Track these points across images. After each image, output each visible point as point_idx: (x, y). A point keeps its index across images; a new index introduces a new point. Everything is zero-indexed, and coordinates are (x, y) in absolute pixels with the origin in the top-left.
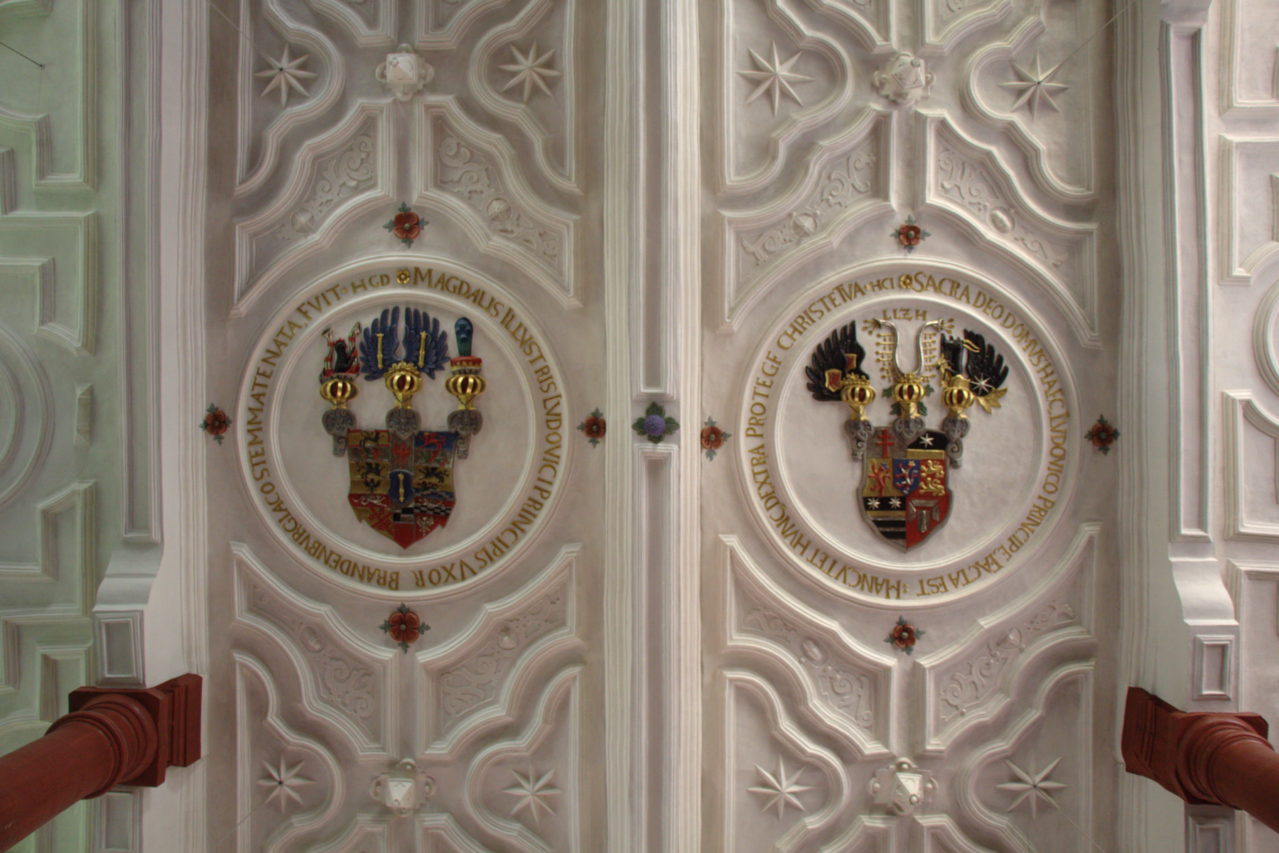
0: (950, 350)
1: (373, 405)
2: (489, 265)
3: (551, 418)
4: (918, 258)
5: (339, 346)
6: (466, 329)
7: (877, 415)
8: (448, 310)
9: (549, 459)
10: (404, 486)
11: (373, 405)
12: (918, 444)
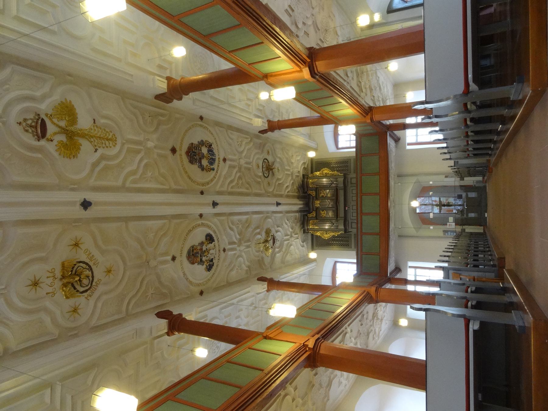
0: (212, 260)
1: (204, 150)
3: (203, 185)
4: (222, 252)
6: (213, 169)
7: (204, 248)
8: (215, 166)
9: (198, 184)
10: (193, 154)
11: (204, 150)
12: (201, 256)
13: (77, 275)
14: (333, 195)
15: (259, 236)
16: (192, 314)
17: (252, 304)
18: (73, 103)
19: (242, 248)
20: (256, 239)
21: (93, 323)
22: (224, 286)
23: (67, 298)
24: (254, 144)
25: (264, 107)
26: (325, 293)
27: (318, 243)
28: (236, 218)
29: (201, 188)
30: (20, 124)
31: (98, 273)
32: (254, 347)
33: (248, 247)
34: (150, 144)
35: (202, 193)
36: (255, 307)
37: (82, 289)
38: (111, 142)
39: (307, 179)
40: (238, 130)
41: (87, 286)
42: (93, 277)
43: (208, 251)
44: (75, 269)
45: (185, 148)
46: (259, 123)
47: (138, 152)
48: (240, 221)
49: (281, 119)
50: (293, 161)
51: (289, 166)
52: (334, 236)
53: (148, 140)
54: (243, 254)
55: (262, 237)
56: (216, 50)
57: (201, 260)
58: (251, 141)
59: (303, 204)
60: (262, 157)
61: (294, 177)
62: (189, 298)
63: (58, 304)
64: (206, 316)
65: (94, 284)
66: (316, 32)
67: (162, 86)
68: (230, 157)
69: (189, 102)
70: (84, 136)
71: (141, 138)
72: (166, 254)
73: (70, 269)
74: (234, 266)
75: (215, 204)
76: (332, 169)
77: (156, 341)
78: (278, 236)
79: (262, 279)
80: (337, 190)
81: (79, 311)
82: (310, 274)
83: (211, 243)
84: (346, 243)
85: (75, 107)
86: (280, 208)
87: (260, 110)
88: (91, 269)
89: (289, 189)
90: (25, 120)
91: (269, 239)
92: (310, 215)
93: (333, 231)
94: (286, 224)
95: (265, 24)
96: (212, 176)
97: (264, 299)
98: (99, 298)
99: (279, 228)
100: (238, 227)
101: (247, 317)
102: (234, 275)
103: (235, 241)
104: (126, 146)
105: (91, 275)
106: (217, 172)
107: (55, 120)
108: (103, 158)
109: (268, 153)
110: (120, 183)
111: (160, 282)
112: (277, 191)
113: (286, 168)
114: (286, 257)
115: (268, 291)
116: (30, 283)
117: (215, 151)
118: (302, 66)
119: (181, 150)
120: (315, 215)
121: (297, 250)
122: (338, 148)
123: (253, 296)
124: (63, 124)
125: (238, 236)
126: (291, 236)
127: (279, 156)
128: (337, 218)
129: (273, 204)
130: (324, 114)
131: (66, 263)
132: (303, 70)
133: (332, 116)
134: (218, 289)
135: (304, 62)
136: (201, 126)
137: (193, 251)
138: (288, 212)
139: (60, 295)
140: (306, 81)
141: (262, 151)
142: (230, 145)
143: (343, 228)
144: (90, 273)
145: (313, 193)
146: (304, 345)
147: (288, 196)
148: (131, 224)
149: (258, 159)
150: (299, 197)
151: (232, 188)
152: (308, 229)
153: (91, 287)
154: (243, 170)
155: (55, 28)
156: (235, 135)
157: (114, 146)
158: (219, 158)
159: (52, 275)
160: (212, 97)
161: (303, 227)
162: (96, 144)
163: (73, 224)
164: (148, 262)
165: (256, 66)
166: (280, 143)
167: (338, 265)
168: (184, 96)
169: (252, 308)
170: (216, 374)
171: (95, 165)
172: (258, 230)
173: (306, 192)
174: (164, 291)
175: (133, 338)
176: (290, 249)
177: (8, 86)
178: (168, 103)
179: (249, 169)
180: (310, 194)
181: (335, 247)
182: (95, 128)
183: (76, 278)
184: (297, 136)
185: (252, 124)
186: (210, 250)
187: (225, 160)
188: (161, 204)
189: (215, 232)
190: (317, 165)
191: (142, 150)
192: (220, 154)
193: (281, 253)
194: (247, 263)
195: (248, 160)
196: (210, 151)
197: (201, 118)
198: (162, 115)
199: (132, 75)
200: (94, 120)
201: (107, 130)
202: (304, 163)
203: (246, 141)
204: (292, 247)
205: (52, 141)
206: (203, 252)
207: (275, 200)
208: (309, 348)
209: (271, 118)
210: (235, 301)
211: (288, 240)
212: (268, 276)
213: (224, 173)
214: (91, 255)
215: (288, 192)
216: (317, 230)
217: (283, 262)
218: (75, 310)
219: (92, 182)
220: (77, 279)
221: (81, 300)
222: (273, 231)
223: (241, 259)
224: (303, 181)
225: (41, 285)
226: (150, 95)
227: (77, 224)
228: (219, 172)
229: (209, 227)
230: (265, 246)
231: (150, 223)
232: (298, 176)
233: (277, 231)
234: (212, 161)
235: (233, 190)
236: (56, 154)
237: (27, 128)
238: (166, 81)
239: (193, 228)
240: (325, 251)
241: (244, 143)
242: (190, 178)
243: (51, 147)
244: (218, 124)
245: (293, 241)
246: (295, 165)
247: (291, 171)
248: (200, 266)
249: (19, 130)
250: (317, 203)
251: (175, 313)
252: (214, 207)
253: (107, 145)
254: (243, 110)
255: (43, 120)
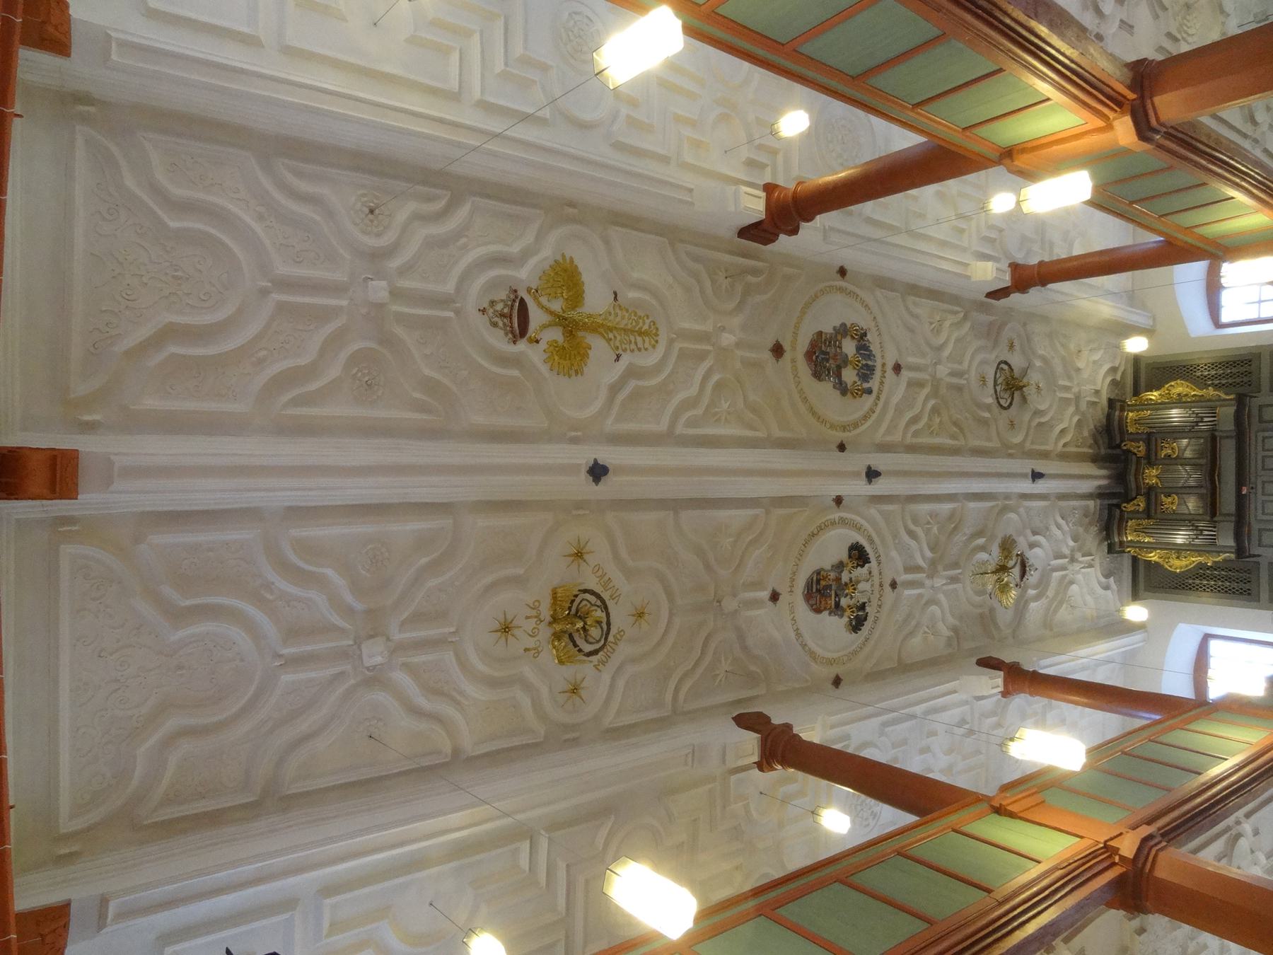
0: (862, 607)
1: (849, 347)
2: (886, 403)
3: (844, 428)
4: (887, 589)
5: (865, 334)
6: (869, 391)
7: (845, 577)
8: (874, 384)
9: (832, 427)
10: (823, 357)
11: (849, 347)
12: (836, 595)
13: (580, 618)
14: (1201, 454)
15: (983, 556)
16: (814, 730)
17: (962, 722)
18: (576, 262)
19: (938, 582)
20: (974, 562)
21: (609, 720)
22: (892, 669)
23: (561, 662)
24: (972, 328)
25: (1001, 231)
26: (1174, 717)
27: (1149, 581)
28: (925, 507)
29: (840, 436)
30: (483, 311)
31: (620, 618)
32: (968, 829)
33: (954, 580)
34: (728, 339)
35: (842, 447)
36: (971, 732)
37: (588, 648)
38: (647, 339)
39: (1122, 410)
40: (934, 294)
41: (598, 641)
42: (609, 624)
43: (853, 584)
44: (575, 604)
45: (803, 344)
46: (988, 273)
47: (702, 356)
48: (933, 515)
49: (1047, 259)
50: (1081, 364)
51: (1070, 378)
52: (1201, 566)
53: (723, 329)
54: (941, 597)
55: (992, 557)
56: (880, 107)
57: (837, 605)
58: (965, 318)
59: (1109, 477)
60: (993, 357)
61: (1083, 406)
62: (807, 691)
63: (545, 672)
64: (847, 737)
65: (611, 638)
66: (1156, 17)
67: (754, 207)
68: (911, 360)
69: (816, 238)
70: (595, 328)
71: (708, 327)
72: (756, 585)
73: (568, 605)
74: (918, 625)
75: (872, 474)
76: (1201, 382)
77: (733, 778)
78: (1036, 557)
79: (989, 663)
80: (1213, 439)
81: (583, 693)
82: (1128, 660)
83: (862, 566)
84: (1241, 585)
85: (581, 269)
86: (1041, 487)
87: (991, 241)
88: (606, 608)
89: (1068, 438)
90: (492, 303)
91: (1011, 563)
92: (1130, 507)
93: (1198, 550)
94: (1059, 527)
95: (1008, 21)
96: (866, 408)
97: (994, 713)
98: (620, 668)
99: (1039, 538)
100: (927, 532)
101: (950, 751)
102: (917, 646)
103: (921, 563)
104: (678, 345)
105: (604, 620)
106: (878, 398)
107: (543, 300)
108: (632, 372)
109: (1011, 346)
110: (663, 426)
111: (745, 648)
112: (1032, 443)
113: (1061, 382)
114: (1055, 611)
115: (1005, 694)
116: (497, 626)
117: (875, 348)
118: (1111, 115)
119: (794, 349)
120: (1142, 505)
121: (1088, 598)
122: (1218, 324)
123: (966, 703)
124: (557, 306)
125: (929, 554)
126: (1073, 560)
127: (1041, 352)
128: (1213, 514)
129: (1024, 476)
130: (1176, 234)
131: (559, 590)
132: (1117, 124)
133: (1203, 238)
134: (876, 676)
135: (1117, 102)
136: (841, 290)
137: (818, 581)
138: (1063, 497)
139: (548, 656)
140: (1125, 152)
141: (996, 343)
142: (911, 330)
143: (1231, 542)
144: (604, 615)
145: (1140, 449)
146: (1106, 847)
147: (1063, 457)
148: (686, 515)
149: (983, 362)
150: (1095, 459)
151: (916, 434)
152: (1121, 543)
153: (604, 645)
154: (943, 391)
155: (546, 113)
156: (924, 307)
157: (654, 347)
158: (884, 365)
159: (534, 613)
160: (870, 221)
161: (1108, 536)
162: (618, 344)
163: (574, 512)
164: (719, 601)
165: (983, 132)
166: (1045, 319)
167: (1214, 645)
168: (804, 225)
169: (961, 731)
170: (871, 878)
171: (615, 389)
172: (981, 541)
173: (1119, 446)
174: (753, 668)
175: (686, 764)
176: (1069, 593)
177: (463, 240)
178: (765, 244)
179: (959, 389)
180: (1129, 451)
181: (1205, 597)
182: (618, 311)
183: (578, 622)
184: (1095, 300)
185: (968, 277)
186: (858, 582)
187: (897, 368)
188: (749, 473)
189: (871, 541)
190: (1151, 373)
191: (709, 352)
192: (885, 354)
193: (1044, 601)
194: (951, 620)
195: (956, 366)
196: (863, 348)
197: (842, 272)
198: (755, 272)
199: (691, 190)
200: (615, 294)
201: (640, 313)
202: (1114, 370)
203: (951, 319)
204: (1074, 587)
205: (537, 342)
206: (842, 587)
207: (1028, 465)
208: (1122, 858)
209: (1020, 258)
210: (918, 709)
211: (1063, 568)
212: (1008, 657)
213: (895, 399)
214: (606, 578)
215: (1065, 445)
216: (1150, 547)
217: (1047, 624)
218: (575, 690)
219: (610, 425)
220: (580, 625)
221: (585, 669)
222: (1022, 545)
223: (934, 608)
224: (1109, 417)
225: (516, 632)
226: (727, 229)
227: (581, 512)
228: (883, 398)
229: (858, 528)
230: (999, 580)
231: (723, 514)
232: (1094, 403)
233: (1032, 546)
234: (866, 373)
235: (915, 440)
236: (544, 369)
237: (496, 319)
238: (763, 195)
239: (820, 529)
240: (1172, 606)
241: (947, 324)
242: (814, 414)
243: (534, 354)
244: (883, 283)
245: (1078, 572)
246: (1085, 375)
247: (1075, 390)
248: (835, 619)
249: (481, 322)
250: (1152, 476)
251: (776, 721)
252: (870, 482)
253: (640, 345)
254: (943, 244)
255: (522, 301)
